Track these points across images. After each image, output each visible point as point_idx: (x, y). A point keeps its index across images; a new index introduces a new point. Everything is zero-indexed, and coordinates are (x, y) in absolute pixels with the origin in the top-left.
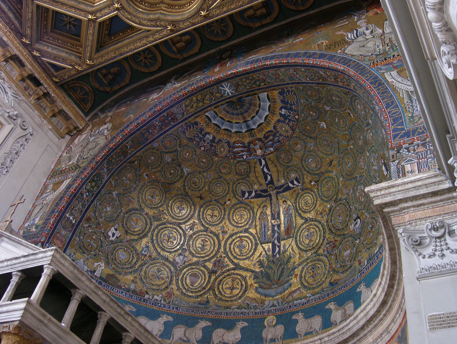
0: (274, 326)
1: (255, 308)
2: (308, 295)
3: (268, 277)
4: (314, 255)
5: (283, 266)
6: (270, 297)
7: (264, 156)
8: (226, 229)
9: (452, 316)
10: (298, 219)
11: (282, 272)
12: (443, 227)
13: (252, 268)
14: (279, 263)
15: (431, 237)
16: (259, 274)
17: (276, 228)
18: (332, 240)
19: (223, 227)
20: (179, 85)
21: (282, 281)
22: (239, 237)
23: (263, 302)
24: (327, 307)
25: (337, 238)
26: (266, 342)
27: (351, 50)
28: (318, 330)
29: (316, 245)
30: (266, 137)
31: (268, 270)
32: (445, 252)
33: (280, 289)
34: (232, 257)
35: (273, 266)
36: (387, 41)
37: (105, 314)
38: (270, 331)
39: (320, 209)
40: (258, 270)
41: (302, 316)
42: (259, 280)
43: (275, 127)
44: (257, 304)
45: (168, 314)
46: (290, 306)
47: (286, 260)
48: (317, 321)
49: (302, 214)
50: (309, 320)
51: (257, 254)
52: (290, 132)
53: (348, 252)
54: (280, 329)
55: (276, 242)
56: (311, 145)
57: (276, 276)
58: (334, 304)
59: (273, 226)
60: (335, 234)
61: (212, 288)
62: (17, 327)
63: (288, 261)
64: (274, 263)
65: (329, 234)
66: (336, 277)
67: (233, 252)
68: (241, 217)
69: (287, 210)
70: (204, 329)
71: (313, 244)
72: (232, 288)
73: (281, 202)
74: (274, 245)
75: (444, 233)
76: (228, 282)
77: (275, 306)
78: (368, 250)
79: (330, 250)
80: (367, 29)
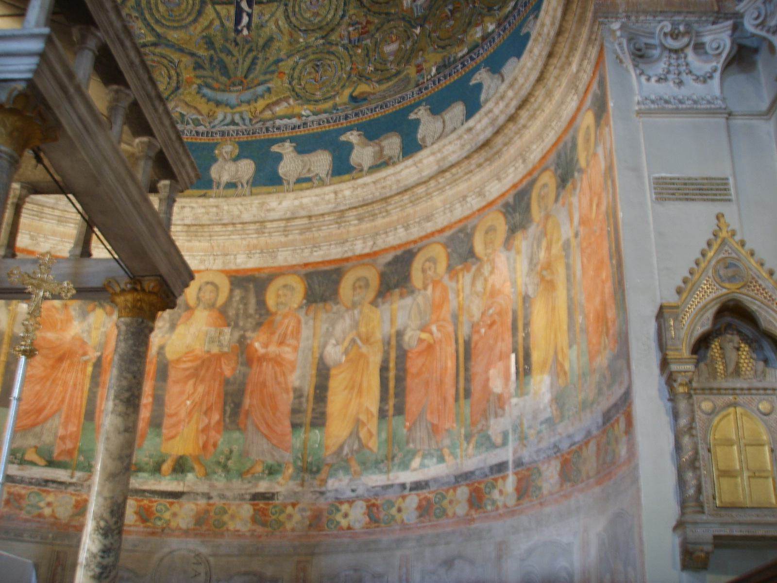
0: (236, 159)
1: (197, 123)
2: (303, 113)
3: (224, 69)
4: (321, 41)
5: (254, 53)
6: (227, 105)
9: (692, 184)
11: (253, 63)
12: (687, 32)
14: (247, 47)
15: (664, 48)
16: (206, 62)
18: (363, 20)
21: (253, 80)
23: (211, 116)
24: (343, 138)
25: (370, 18)
26: (218, 188)
28: (323, 175)
29: (327, 24)
31: (223, 56)
32: (684, 77)
33: (247, 95)
34: (152, 22)
35: (235, 51)
37: (128, 91)
38: (227, 167)
40: (201, 53)
41: (291, 149)
42: (205, 73)
44: (200, 117)
46: (267, 130)
47: (261, 42)
48: (322, 161)
50: (306, 157)
51: (204, 22)
53: (393, 47)
54: (246, 168)
57: (240, 69)
58: (359, 135)
60: (369, 10)
62: (22, 95)
64: (237, 44)
65: (355, 8)
66: (363, 88)
67: (154, 11)
71: (319, 22)
74: (239, 12)
75: (687, 45)
77: (237, 124)
78: (440, 50)
79: (355, 36)
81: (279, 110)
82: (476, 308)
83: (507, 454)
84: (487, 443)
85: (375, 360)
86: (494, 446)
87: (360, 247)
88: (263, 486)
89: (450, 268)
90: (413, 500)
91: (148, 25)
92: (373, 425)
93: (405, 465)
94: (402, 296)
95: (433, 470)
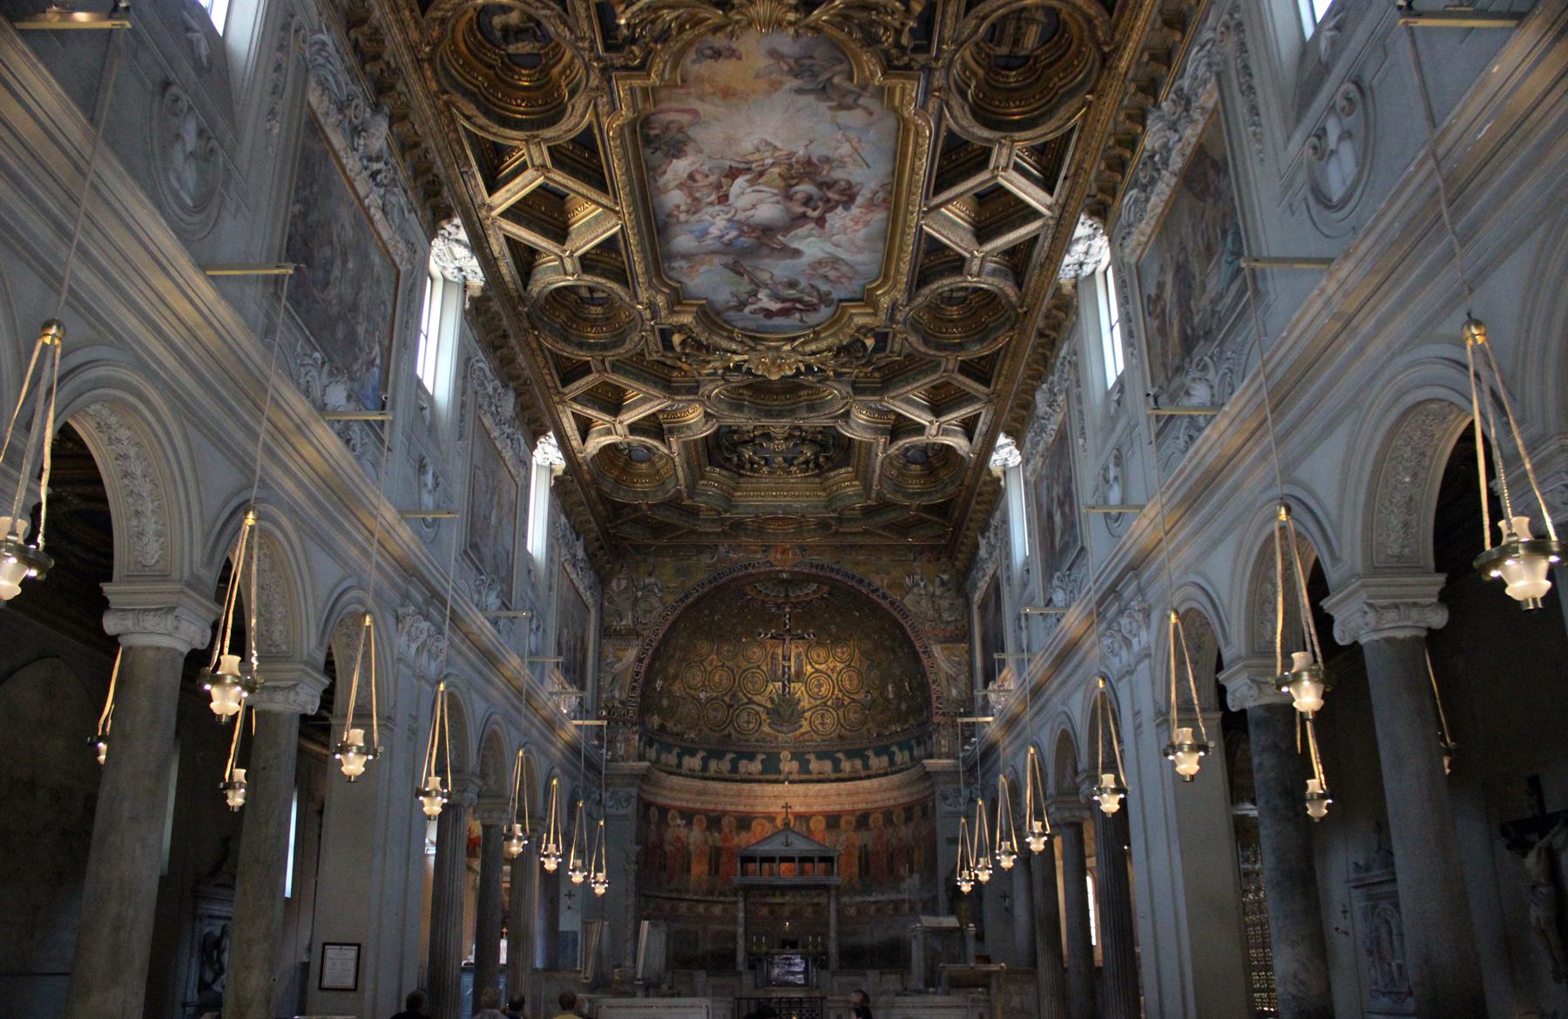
3: (779, 714)
10: (809, 667)
23: (776, 738)
27: (908, 601)
33: (792, 728)
39: (831, 666)
40: (770, 706)
48: (827, 766)
56: (838, 619)
61: (731, 722)
63: (798, 703)
69: (798, 656)
72: (749, 722)
74: (784, 686)
76: (744, 716)
81: (807, 737)
82: (894, 842)
83: (905, 896)
84: (899, 891)
85: (856, 854)
87: (847, 807)
88: (816, 900)
89: (884, 824)
90: (873, 908)
92: (857, 879)
93: (870, 895)
95: (881, 898)
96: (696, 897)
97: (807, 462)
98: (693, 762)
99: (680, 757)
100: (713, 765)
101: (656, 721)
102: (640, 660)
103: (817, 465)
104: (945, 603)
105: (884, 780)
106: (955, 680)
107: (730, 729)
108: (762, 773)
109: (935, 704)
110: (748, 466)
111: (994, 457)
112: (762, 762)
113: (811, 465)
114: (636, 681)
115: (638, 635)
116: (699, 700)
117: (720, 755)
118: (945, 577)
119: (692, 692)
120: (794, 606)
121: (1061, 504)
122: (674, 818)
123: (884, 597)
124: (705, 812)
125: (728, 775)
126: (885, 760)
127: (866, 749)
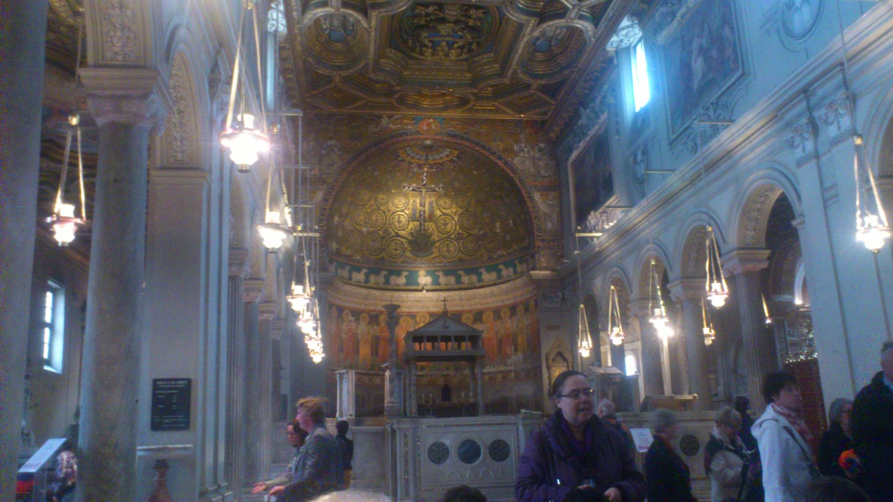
7: (427, 172)
8: (390, 208)
13: (406, 236)
17: (422, 213)
19: (388, 207)
20: (394, 127)
22: (399, 215)
24: (458, 272)
27: (516, 161)
30: (434, 164)
36: (536, 166)
43: (444, 162)
45: (366, 268)
49: (442, 209)
51: (410, 228)
52: (452, 167)
55: (422, 222)
56: (461, 177)
59: (420, 211)
61: (384, 250)
63: (430, 237)
68: (400, 201)
69: (431, 204)
70: (385, 276)
72: (396, 250)
73: (427, 196)
74: (421, 224)
80: (526, 147)
81: (437, 260)
84: (506, 365)
86: (508, 366)
87: (466, 308)
88: (446, 373)
89: (494, 319)
91: (393, 230)
94: (481, 323)
95: (492, 370)
96: (363, 371)
97: (462, 48)
98: (359, 277)
99: (350, 272)
100: (372, 279)
101: (334, 246)
102: (326, 200)
103: (470, 51)
104: (542, 164)
105: (495, 289)
106: (550, 216)
107: (383, 254)
108: (405, 285)
109: (536, 233)
110: (418, 49)
111: (614, 39)
112: (406, 276)
113: (465, 50)
114: (323, 215)
115: (324, 182)
116: (362, 233)
117: (377, 272)
118: (542, 145)
119: (357, 227)
120: (431, 166)
121: (703, 51)
122: (347, 314)
123: (500, 158)
124: (369, 313)
125: (383, 286)
126: (493, 276)
127: (480, 268)
